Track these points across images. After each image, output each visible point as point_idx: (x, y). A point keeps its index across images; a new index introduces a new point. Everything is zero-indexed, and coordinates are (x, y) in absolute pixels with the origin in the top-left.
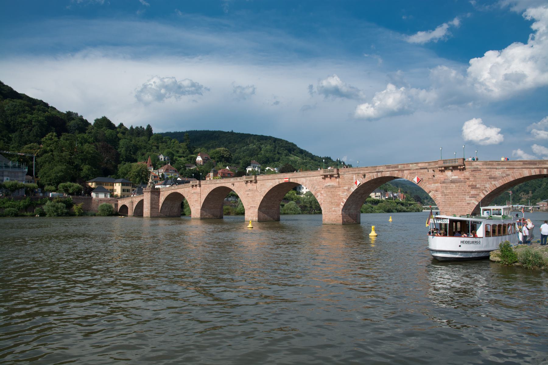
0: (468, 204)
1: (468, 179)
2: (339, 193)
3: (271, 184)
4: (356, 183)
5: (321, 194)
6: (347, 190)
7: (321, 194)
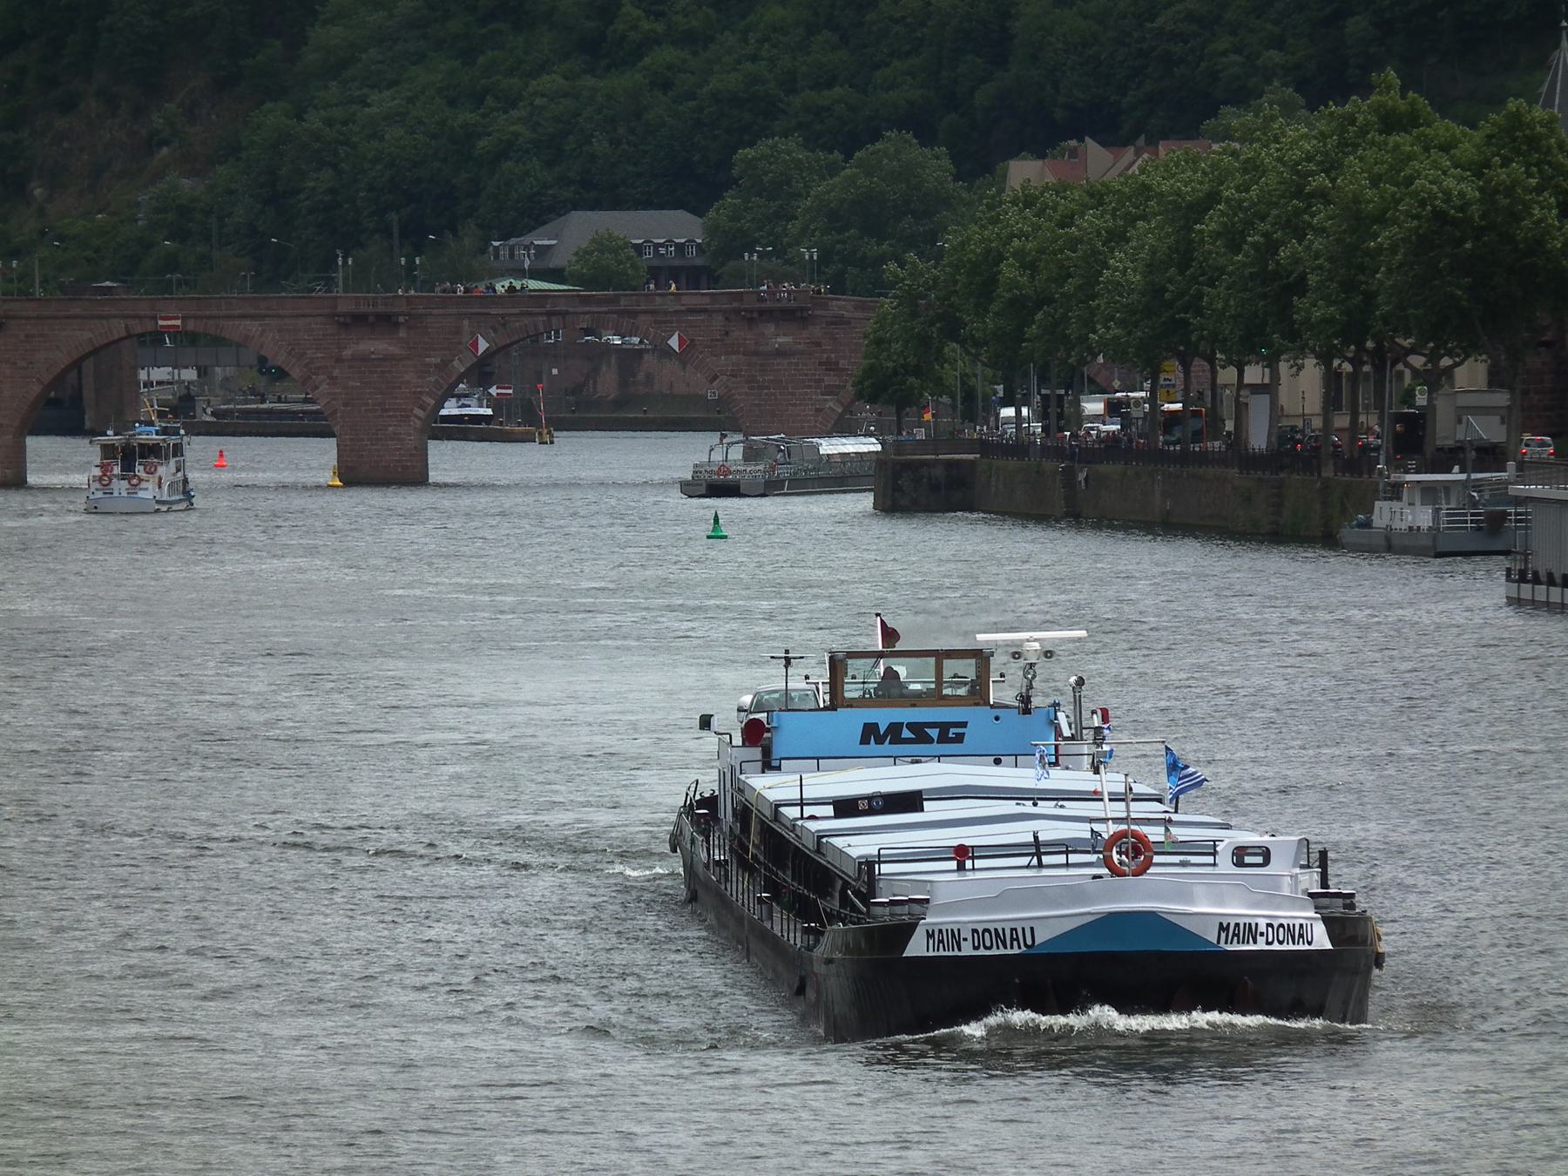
0: (818, 410)
1: (818, 344)
2: (407, 377)
3: (87, 335)
4: (475, 345)
5: (332, 378)
6: (436, 366)
7: (332, 378)
